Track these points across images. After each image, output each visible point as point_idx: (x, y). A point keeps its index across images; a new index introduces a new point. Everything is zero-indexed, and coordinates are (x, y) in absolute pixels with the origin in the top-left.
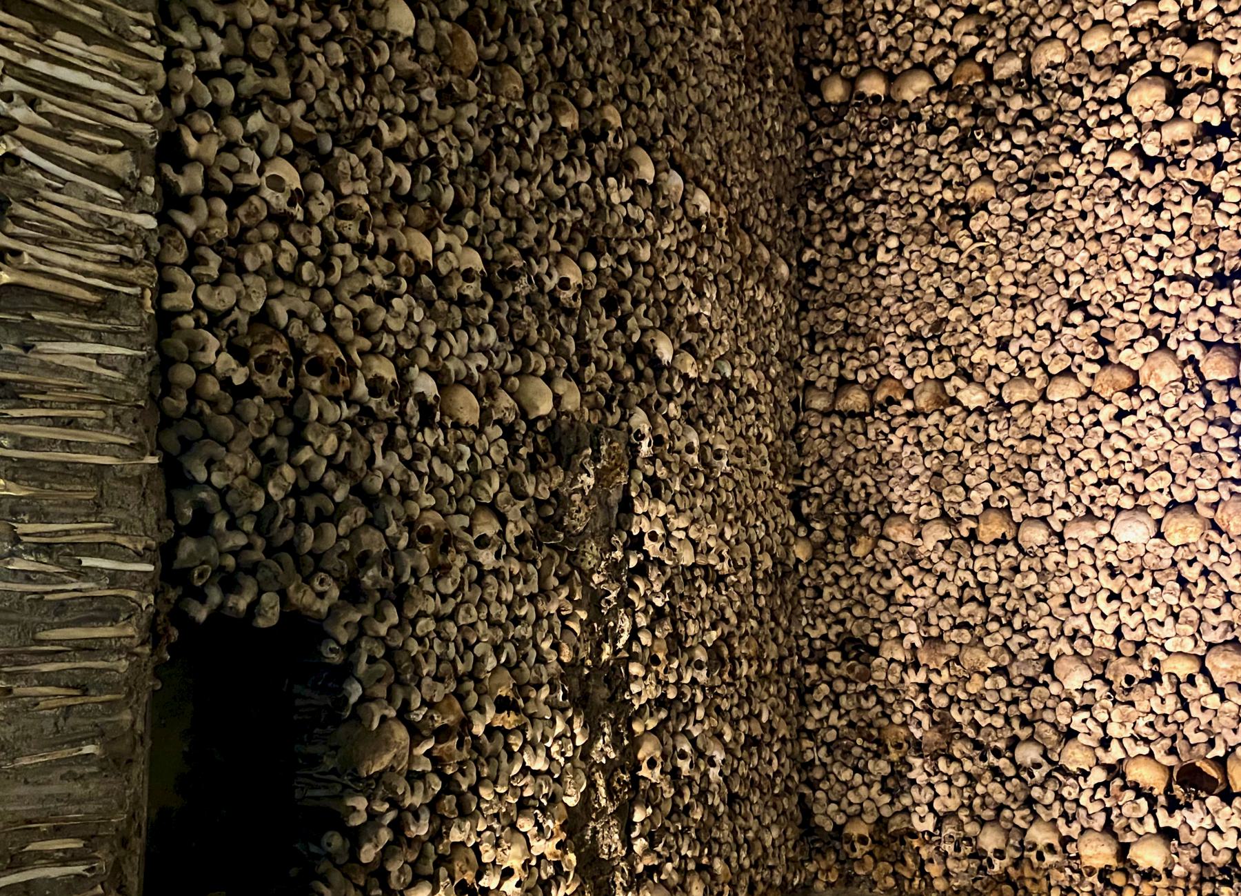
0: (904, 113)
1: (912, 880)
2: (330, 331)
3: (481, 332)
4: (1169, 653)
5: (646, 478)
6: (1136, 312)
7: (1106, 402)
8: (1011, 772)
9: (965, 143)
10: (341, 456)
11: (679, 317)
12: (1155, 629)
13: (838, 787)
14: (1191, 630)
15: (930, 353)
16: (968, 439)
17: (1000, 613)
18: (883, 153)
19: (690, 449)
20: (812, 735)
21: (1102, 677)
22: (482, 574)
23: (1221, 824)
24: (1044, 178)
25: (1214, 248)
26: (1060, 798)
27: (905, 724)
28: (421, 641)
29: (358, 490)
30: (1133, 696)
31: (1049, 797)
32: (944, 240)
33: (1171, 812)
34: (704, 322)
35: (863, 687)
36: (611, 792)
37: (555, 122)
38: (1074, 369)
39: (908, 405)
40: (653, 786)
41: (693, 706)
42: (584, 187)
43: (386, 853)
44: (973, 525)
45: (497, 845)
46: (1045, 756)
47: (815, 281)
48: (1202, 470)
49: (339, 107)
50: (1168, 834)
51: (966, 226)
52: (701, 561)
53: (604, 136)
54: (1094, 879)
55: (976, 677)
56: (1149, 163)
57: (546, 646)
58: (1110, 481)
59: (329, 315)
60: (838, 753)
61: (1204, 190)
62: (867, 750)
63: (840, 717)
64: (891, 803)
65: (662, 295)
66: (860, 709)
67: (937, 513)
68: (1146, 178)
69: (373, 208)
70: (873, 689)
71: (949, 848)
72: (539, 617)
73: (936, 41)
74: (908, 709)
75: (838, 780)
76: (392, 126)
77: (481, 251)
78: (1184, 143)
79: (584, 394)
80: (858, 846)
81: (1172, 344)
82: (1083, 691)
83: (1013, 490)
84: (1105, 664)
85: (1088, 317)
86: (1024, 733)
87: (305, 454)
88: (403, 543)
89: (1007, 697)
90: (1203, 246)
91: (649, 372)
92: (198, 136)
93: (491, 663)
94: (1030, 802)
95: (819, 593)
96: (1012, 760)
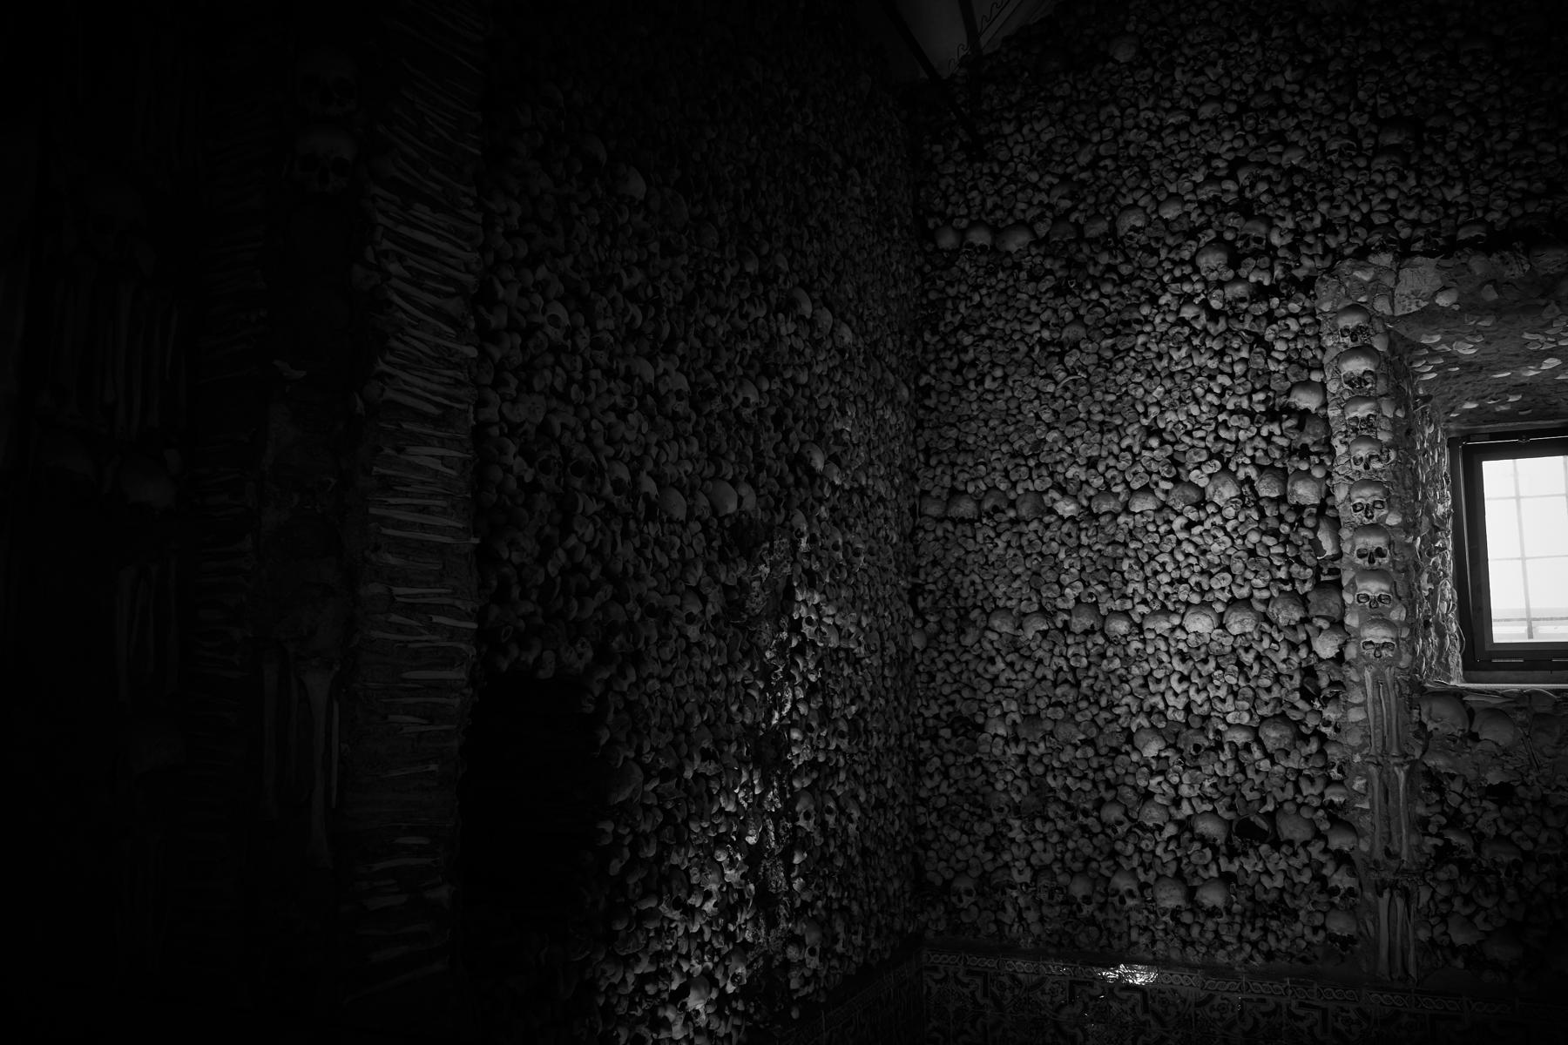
0: (1008, 262)
1: (1012, 925)
2: (588, 442)
3: (688, 442)
4: (1229, 725)
5: (804, 571)
6: (1203, 439)
7: (1179, 514)
8: (1097, 829)
9: (1060, 291)
10: (596, 544)
11: (828, 432)
12: (1219, 706)
13: (947, 846)
14: (1247, 705)
15: (1030, 469)
16: (1063, 544)
17: (1089, 693)
18: (989, 295)
19: (836, 547)
20: (924, 802)
21: (1174, 746)
22: (689, 645)
23: (1270, 866)
24: (1127, 324)
25: (1266, 388)
26: (1140, 851)
27: (1005, 791)
28: (650, 696)
29: (606, 572)
30: (1201, 762)
31: (1130, 849)
32: (1042, 373)
33: (1231, 861)
34: (846, 437)
35: (970, 759)
37: (742, 269)
38: (1153, 486)
39: (1012, 514)
40: (808, 834)
42: (761, 321)
43: (627, 869)
44: (1066, 617)
45: (701, 871)
46: (1126, 814)
47: (930, 403)
48: (1256, 572)
49: (596, 259)
50: (1227, 878)
51: (1061, 362)
52: (844, 645)
53: (776, 279)
54: (1167, 918)
55: (1069, 748)
56: (1214, 316)
57: (734, 708)
58: (1182, 581)
59: (587, 428)
60: (947, 818)
61: (1259, 339)
62: (972, 814)
63: (949, 786)
64: (994, 860)
65: (815, 413)
66: (967, 778)
67: (1036, 607)
68: (1212, 328)
69: (616, 339)
70: (979, 761)
71: (1044, 896)
72: (729, 684)
73: (1035, 202)
74: (1009, 778)
75: (947, 841)
76: (630, 274)
77: (687, 375)
78: (1243, 300)
79: (759, 496)
80: (965, 898)
81: (1233, 467)
82: (1158, 758)
83: (1100, 588)
84: (1177, 735)
85: (1163, 442)
86: (1109, 795)
87: (572, 541)
88: (637, 617)
89: (1095, 765)
90: (1258, 386)
91: (806, 479)
92: (504, 284)
93: (697, 720)
94: (1113, 854)
95: (932, 678)
96: (1099, 819)
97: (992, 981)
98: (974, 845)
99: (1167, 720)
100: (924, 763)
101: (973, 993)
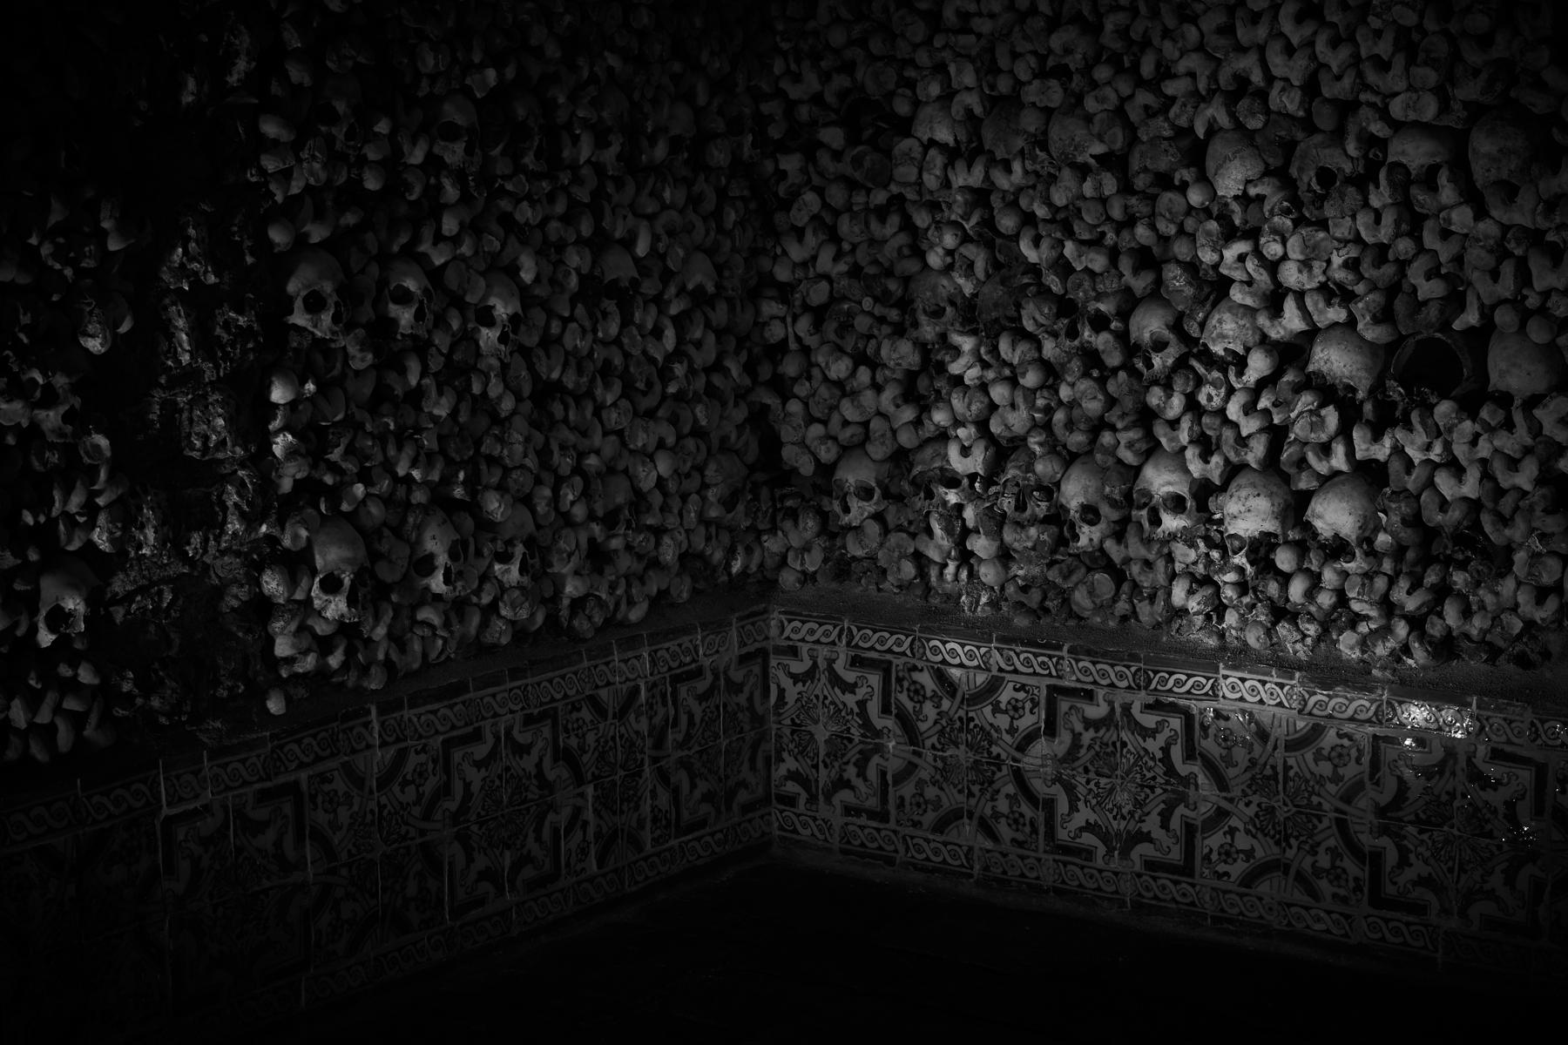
1: (945, 565)
8: (1114, 359)
13: (824, 392)
20: (784, 292)
23: (1460, 451)
31: (1177, 404)
35: (880, 197)
36: (204, 342)
40: (319, 343)
41: (433, 208)
50: (1370, 475)
54: (1240, 559)
55: (1066, 173)
60: (830, 327)
62: (882, 320)
63: (837, 258)
64: (917, 423)
66: (872, 242)
70: (898, 201)
75: (826, 379)
80: (854, 504)
82: (1244, 199)
86: (1140, 284)
96: (1123, 337)
97: (899, 680)
98: (878, 388)
99: (1267, 112)
100: (786, 205)
101: (862, 704)
